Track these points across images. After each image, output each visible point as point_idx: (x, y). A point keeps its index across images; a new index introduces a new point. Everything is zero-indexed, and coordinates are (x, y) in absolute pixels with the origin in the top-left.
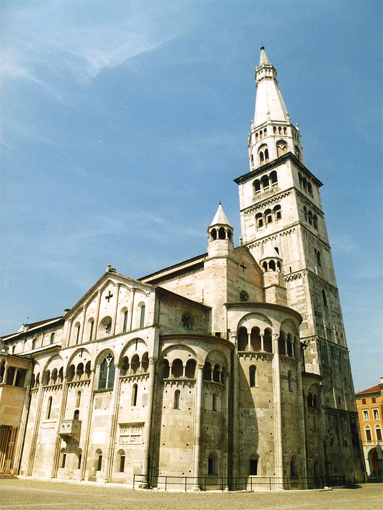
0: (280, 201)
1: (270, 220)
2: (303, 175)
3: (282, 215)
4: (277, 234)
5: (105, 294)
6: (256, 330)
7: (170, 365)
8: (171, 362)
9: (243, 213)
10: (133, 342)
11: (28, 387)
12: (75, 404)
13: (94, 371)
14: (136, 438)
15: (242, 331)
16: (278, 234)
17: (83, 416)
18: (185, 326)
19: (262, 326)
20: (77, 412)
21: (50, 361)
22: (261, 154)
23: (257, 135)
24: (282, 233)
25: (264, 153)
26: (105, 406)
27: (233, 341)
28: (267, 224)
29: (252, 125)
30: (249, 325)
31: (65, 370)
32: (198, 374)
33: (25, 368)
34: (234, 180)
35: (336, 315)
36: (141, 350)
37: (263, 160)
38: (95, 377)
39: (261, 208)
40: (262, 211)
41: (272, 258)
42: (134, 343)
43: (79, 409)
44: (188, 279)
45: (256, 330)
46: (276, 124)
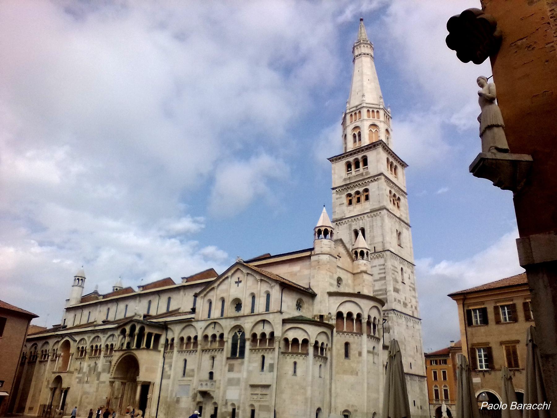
0: (369, 185)
1: (359, 201)
2: (391, 160)
5: (235, 279)
6: (350, 314)
7: (290, 343)
8: (290, 339)
9: (334, 191)
10: (260, 322)
11: (162, 350)
13: (227, 341)
15: (340, 315)
16: (365, 216)
17: (216, 376)
18: (297, 309)
19: (355, 311)
20: (211, 374)
21: (184, 329)
22: (354, 136)
23: (351, 115)
24: (369, 215)
27: (333, 322)
29: (348, 105)
30: (345, 311)
31: (200, 338)
32: (311, 350)
33: (160, 333)
34: (328, 159)
35: (411, 289)
36: (267, 330)
38: (228, 346)
40: (353, 192)
41: (363, 248)
43: (214, 371)
44: (296, 268)
45: (350, 314)
46: (370, 108)
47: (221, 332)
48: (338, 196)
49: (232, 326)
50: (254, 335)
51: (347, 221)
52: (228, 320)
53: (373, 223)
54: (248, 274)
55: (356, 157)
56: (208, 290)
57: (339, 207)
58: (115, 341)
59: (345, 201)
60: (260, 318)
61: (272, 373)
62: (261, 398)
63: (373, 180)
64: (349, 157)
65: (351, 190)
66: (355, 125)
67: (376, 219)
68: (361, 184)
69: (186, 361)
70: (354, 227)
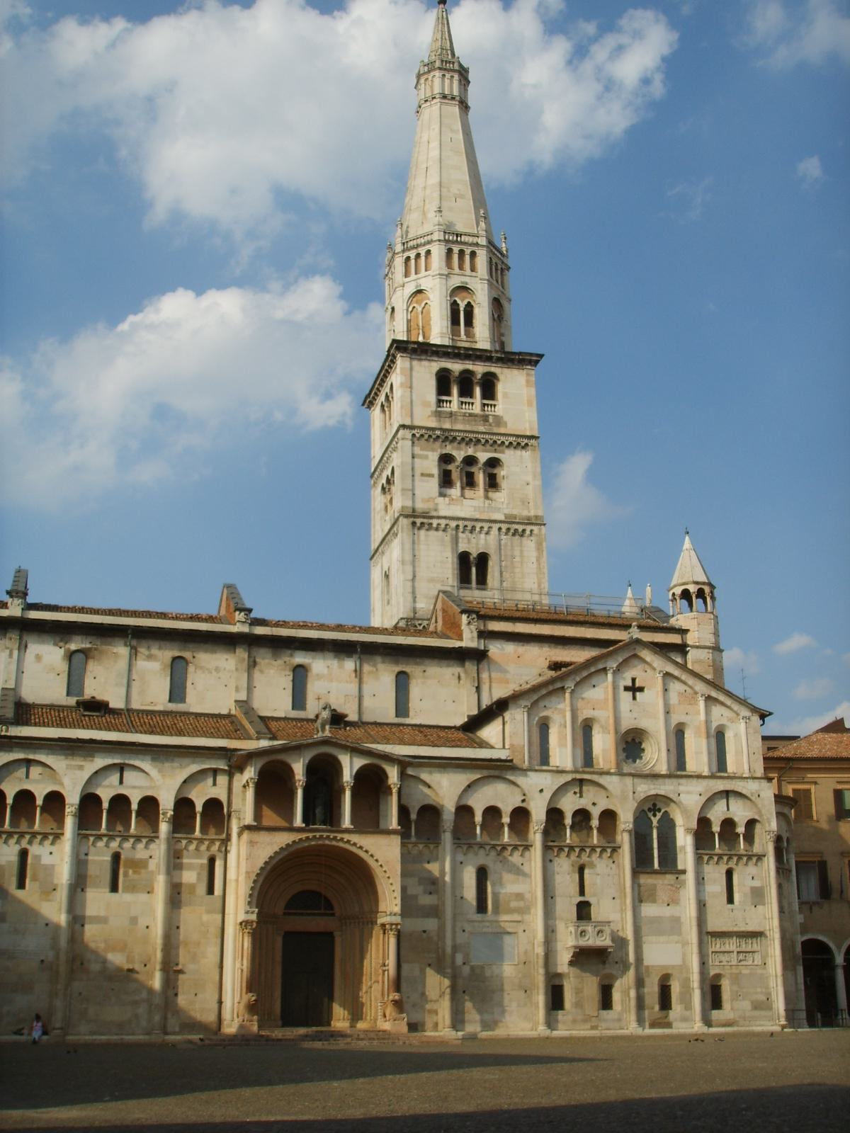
0: (503, 452)
1: (470, 482)
3: (504, 484)
4: (493, 525)
12: (575, 888)
14: (747, 955)
16: (496, 526)
23: (450, 251)
24: (504, 527)
25: (462, 309)
26: (666, 899)
28: (463, 488)
37: (458, 324)
39: (455, 444)
40: (459, 455)
42: (723, 798)
47: (603, 804)
49: (643, 796)
50: (704, 822)
52: (629, 780)
53: (512, 549)
56: (544, 692)
58: (134, 787)
59: (435, 471)
60: (721, 785)
61: (760, 908)
62: (740, 961)
65: (453, 448)
68: (483, 441)
70: (462, 547)
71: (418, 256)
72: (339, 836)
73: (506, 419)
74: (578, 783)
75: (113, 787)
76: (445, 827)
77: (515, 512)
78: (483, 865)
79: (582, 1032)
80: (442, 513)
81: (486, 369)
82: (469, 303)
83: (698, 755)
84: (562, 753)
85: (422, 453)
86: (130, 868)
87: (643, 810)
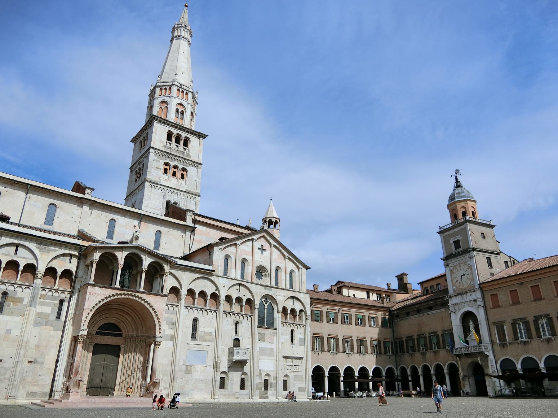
0: (188, 167)
1: (174, 174)
16: (182, 193)
22: (177, 110)
23: (178, 90)
24: (185, 194)
40: (172, 164)
43: (240, 338)
47: (249, 296)
48: (156, 158)
50: (285, 309)
51: (162, 189)
53: (187, 203)
54: (275, 246)
55: (180, 133)
57: (155, 170)
58: (23, 258)
59: (163, 167)
63: (193, 164)
64: (173, 128)
65: (169, 161)
66: (182, 103)
67: (190, 201)
69: (195, 320)
70: (168, 198)
71: (166, 89)
72: (137, 294)
73: (190, 155)
74: (239, 285)
75: (10, 256)
76: (182, 298)
77: (190, 189)
78: (196, 318)
79: (233, 400)
80: (161, 184)
81: (186, 135)
82: (182, 111)
83: (284, 281)
84: (235, 272)
85: (157, 159)
86: (12, 302)
87: (262, 301)
